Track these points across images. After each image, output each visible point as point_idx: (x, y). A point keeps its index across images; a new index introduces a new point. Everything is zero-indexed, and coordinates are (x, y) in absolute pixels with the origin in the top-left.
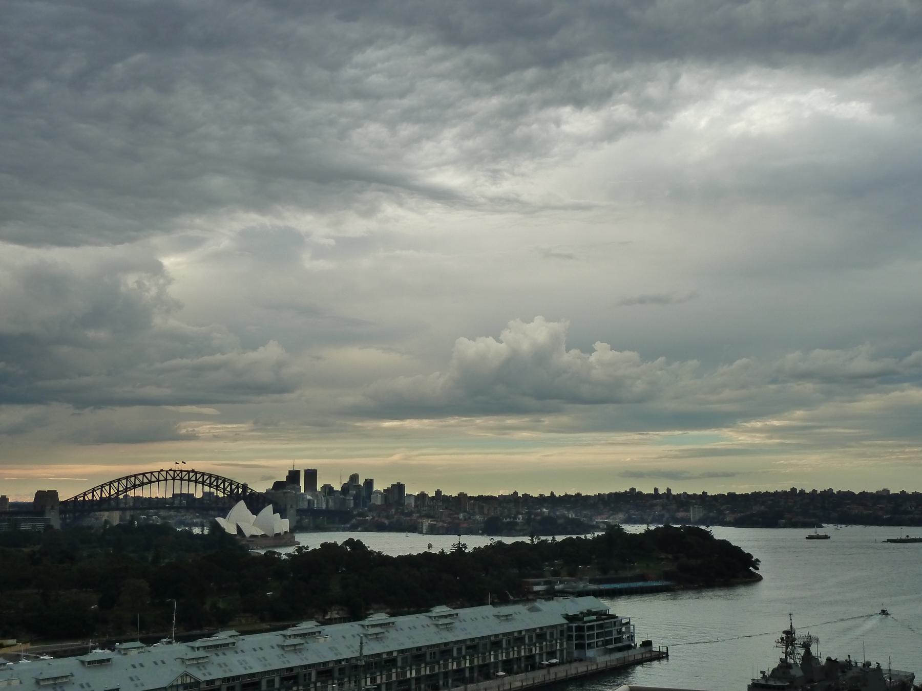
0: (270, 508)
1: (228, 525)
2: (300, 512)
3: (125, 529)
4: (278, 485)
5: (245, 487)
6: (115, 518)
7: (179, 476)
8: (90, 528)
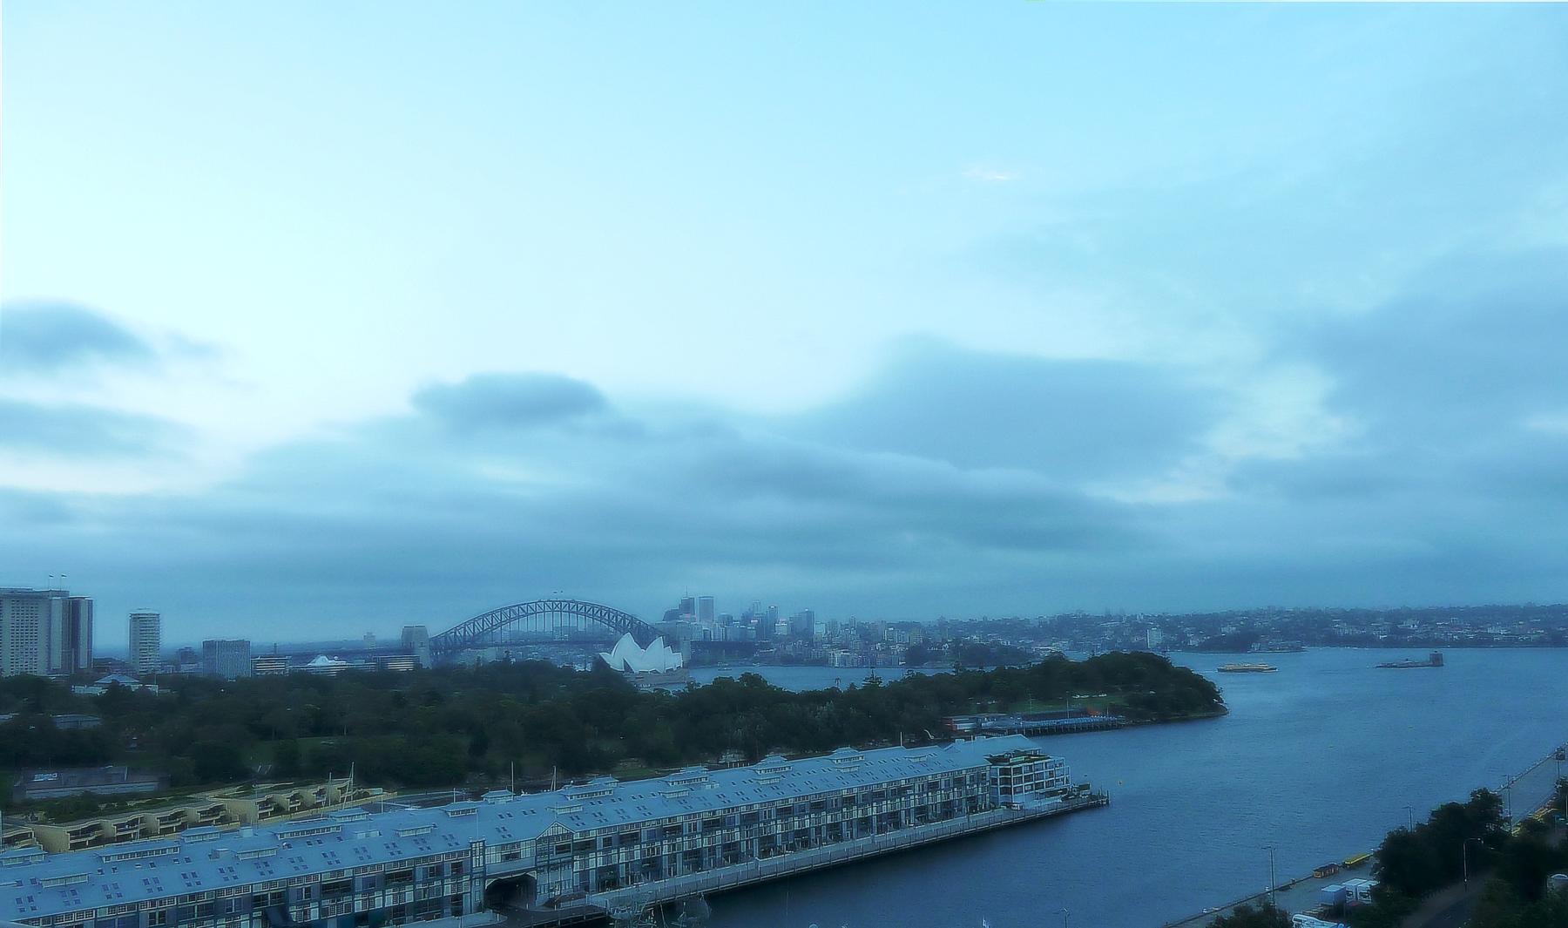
0: (658, 644)
1: (614, 660)
2: (695, 644)
3: (503, 666)
4: (671, 615)
5: (633, 619)
6: (490, 655)
7: (558, 606)
8: (462, 666)
